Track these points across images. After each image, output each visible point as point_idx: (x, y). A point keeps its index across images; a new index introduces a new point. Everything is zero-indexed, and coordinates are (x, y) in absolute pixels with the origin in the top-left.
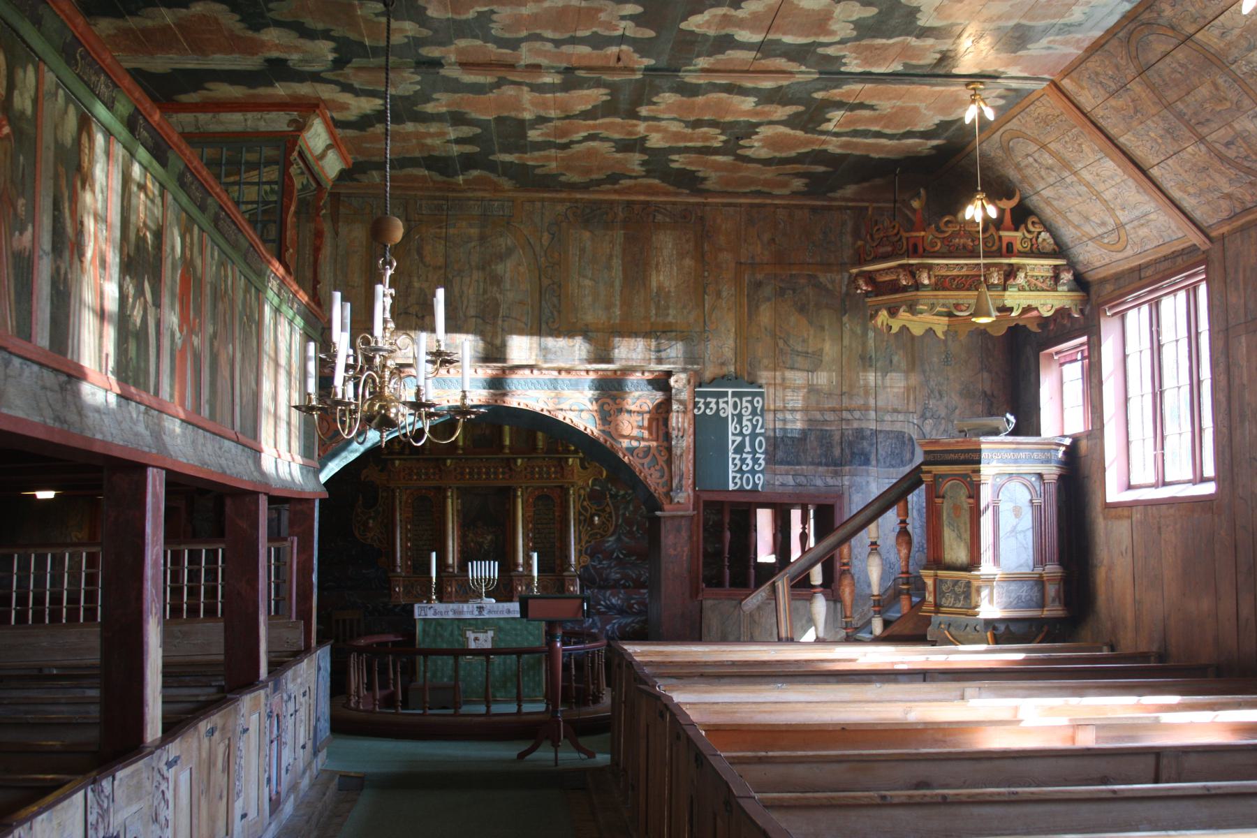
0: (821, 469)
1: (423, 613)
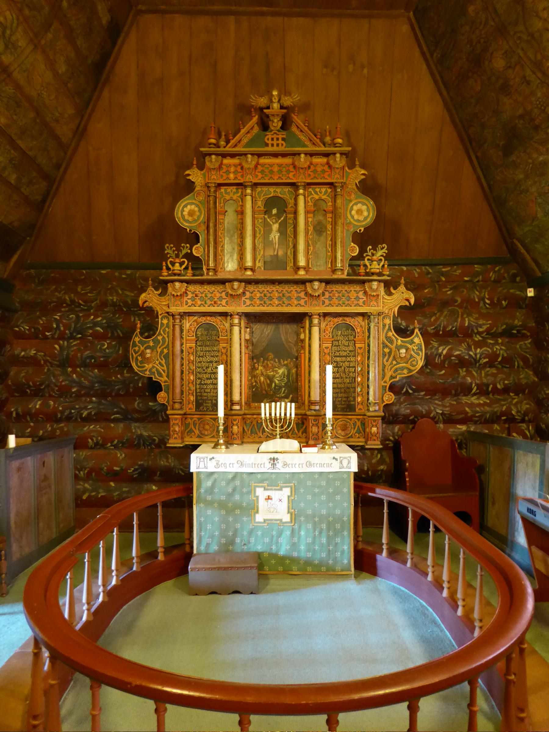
1: (202, 465)
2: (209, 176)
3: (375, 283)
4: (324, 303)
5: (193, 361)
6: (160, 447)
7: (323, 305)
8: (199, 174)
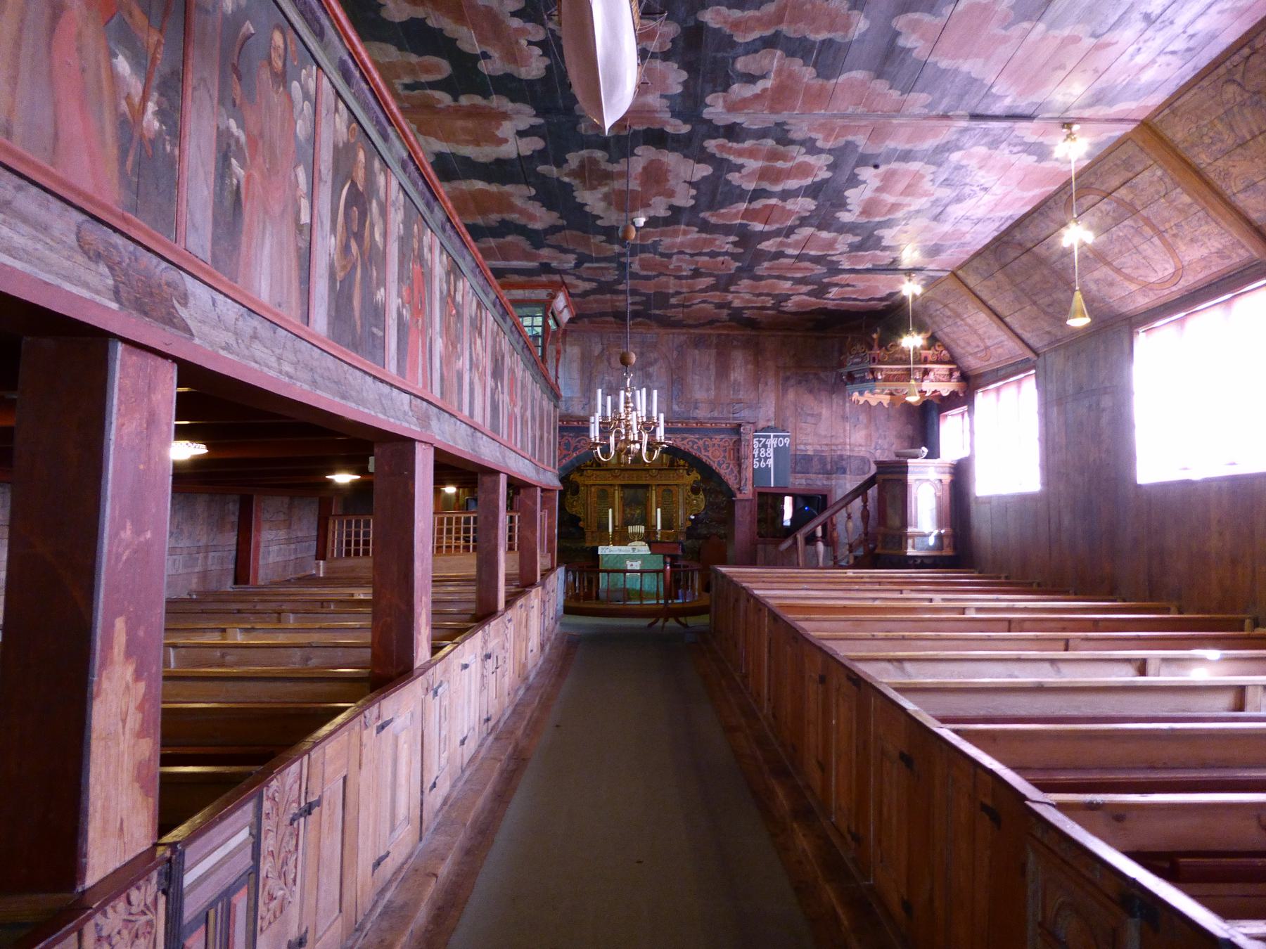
0: (820, 476)
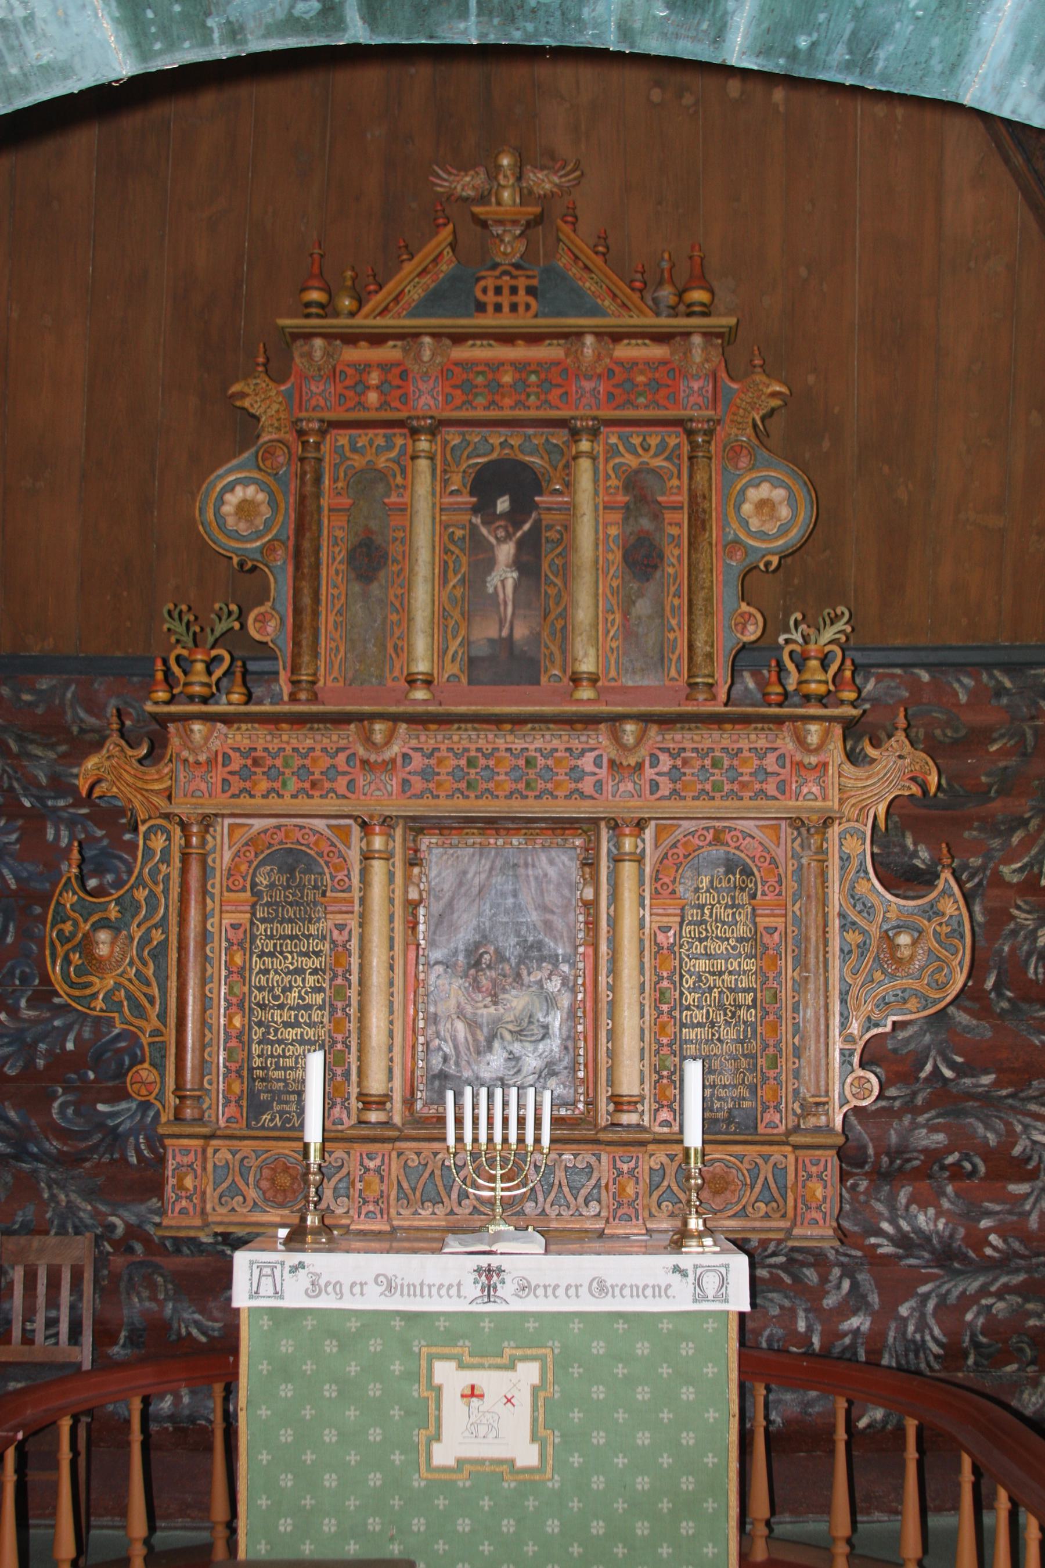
2: (305, 398)
3: (814, 728)
4: (655, 786)
5: (243, 968)
6: (131, 1250)
7: (652, 793)
8: (273, 393)
